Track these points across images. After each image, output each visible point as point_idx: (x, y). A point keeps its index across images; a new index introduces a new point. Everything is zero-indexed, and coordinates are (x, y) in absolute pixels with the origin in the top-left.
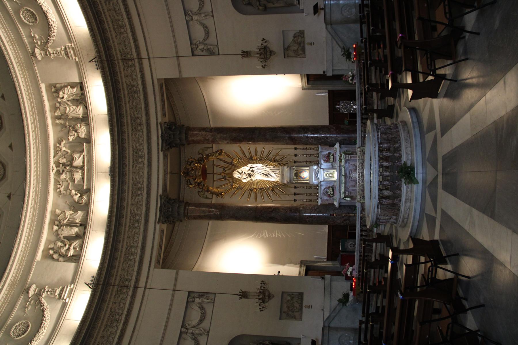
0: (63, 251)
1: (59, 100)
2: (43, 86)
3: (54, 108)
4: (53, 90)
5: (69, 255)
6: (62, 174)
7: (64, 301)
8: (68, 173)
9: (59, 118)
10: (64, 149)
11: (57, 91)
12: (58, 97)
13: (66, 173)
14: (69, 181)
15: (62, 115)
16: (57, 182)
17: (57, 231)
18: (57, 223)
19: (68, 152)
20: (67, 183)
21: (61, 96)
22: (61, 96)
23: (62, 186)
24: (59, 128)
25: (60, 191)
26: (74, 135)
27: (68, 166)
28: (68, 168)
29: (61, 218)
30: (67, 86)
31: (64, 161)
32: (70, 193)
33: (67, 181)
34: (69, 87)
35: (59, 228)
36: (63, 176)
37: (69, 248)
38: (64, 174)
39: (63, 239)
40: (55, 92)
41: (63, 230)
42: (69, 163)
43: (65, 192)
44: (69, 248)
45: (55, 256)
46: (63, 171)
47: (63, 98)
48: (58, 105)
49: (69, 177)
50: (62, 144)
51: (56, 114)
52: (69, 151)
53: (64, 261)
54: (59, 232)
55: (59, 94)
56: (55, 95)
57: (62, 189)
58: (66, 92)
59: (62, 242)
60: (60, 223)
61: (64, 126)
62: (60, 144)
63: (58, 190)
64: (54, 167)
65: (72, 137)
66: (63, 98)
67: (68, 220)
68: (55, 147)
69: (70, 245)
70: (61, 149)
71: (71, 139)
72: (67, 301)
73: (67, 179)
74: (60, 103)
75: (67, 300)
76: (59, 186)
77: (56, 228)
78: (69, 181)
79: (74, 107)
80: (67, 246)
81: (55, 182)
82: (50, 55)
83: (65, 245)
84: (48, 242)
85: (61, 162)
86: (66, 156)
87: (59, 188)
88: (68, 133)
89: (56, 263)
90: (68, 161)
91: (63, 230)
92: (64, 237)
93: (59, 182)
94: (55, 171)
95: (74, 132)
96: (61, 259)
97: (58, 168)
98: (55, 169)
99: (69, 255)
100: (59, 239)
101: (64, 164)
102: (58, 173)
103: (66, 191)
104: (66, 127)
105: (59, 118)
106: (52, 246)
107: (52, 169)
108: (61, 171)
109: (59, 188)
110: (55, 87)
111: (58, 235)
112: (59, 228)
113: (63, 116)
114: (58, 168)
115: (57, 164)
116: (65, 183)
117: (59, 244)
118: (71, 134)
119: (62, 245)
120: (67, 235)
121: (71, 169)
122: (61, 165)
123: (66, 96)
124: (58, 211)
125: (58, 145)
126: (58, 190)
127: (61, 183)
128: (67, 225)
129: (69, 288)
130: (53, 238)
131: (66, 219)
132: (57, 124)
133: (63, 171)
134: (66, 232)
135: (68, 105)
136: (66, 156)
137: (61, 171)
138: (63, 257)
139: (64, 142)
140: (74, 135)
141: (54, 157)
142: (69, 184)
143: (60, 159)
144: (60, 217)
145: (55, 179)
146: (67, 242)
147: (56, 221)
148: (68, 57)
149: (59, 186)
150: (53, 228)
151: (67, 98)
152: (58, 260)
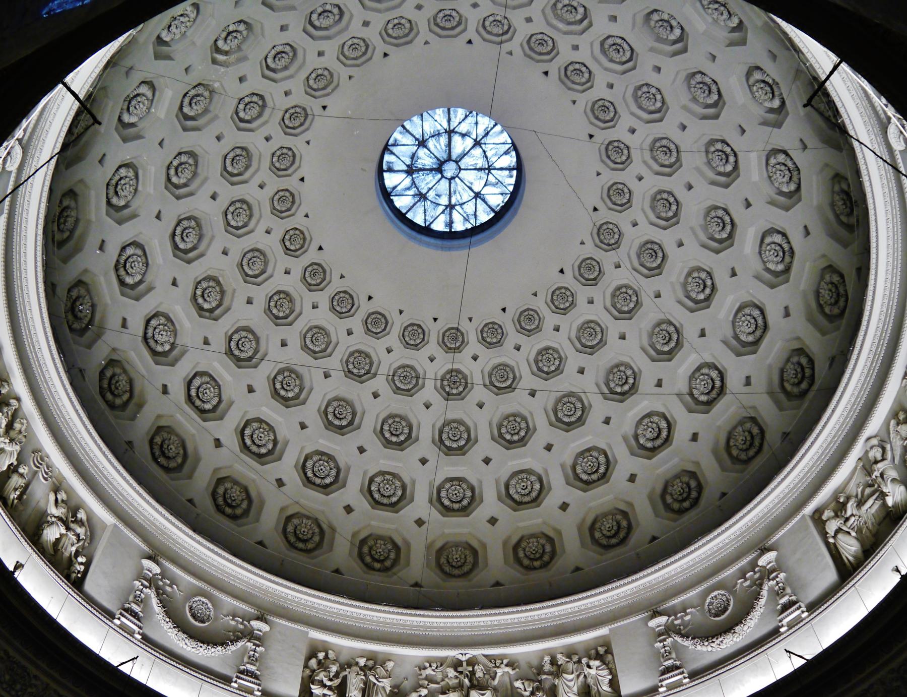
0: (321, 676)
1: (584, 661)
2: (603, 631)
3: (570, 653)
4: (600, 649)
5: (312, 686)
6: (456, 670)
7: (235, 679)
8: (457, 681)
9: (553, 662)
10: (499, 672)
11: (598, 657)
12: (590, 658)
13: (456, 677)
14: (442, 683)
15: (559, 666)
16: (442, 662)
17: (357, 664)
18: (371, 663)
19: (493, 679)
20: (439, 680)
21: (592, 663)
22: (592, 663)
23: (434, 670)
24: (535, 662)
25: (425, 668)
26: (525, 690)
27: (470, 681)
28: (466, 681)
29: (378, 671)
30: (611, 673)
31: (479, 674)
32: (422, 686)
33: (443, 680)
34: (610, 677)
35: (361, 669)
36: (451, 673)
37: (324, 686)
38: (455, 673)
39: (341, 675)
40: (597, 653)
41: (358, 674)
42: (476, 683)
43: (424, 676)
44: (324, 686)
45: (313, 663)
46: (461, 673)
47: (589, 667)
48: (575, 658)
49: (450, 683)
50: (508, 669)
51: (559, 656)
52: (496, 682)
53: (302, 678)
54: (356, 669)
55: (596, 659)
56: (593, 652)
57: (429, 671)
58: (600, 672)
59: (337, 675)
60: (370, 669)
61: (540, 670)
62: (506, 665)
63: (427, 665)
64: (468, 656)
65: (522, 687)
66: (589, 667)
67: (375, 684)
68: (502, 657)
69: (330, 688)
70: (498, 667)
71: (518, 684)
72: (233, 684)
73: (447, 680)
74: (579, 662)
75: (235, 685)
76: (434, 665)
77: (362, 662)
78: (442, 683)
79: (575, 689)
80: (329, 683)
81: (442, 658)
82: (660, 641)
83: (331, 680)
84: (339, 650)
85: (476, 667)
86: (487, 676)
87: (430, 666)
88: (528, 680)
89: (302, 664)
90: (478, 681)
91: (358, 674)
92: (345, 679)
93: (441, 665)
94: (460, 657)
95: (531, 689)
96: (308, 672)
97: (465, 664)
98: (463, 658)
99: (312, 686)
100: (342, 668)
101: (473, 673)
102: (457, 664)
103: (426, 678)
104: (539, 674)
105: (553, 662)
106: (331, 655)
107: (463, 652)
108: (460, 669)
109: (430, 666)
110: (606, 652)
111: (349, 666)
112: (361, 669)
113: (558, 670)
114: (465, 664)
115: (472, 662)
116: (439, 676)
117: (334, 669)
118: (526, 683)
119: (332, 675)
120: (348, 682)
121: (465, 688)
122: (470, 669)
123: (593, 672)
124: (390, 665)
125: (505, 661)
126: (427, 665)
127: (440, 669)
128: (366, 683)
129: (256, 687)
130: (343, 658)
131: (377, 679)
132: (542, 659)
133: (461, 673)
134: (354, 681)
135: (578, 676)
136: (487, 676)
137: (460, 669)
138: (310, 676)
139: (512, 672)
140: (525, 690)
141: (485, 656)
142: (438, 683)
143: (481, 667)
144: (380, 671)
145: (447, 658)
146: (337, 682)
147: (375, 662)
148: (663, 673)
149: (434, 665)
150: (362, 657)
151: (589, 674)
152: (306, 666)
